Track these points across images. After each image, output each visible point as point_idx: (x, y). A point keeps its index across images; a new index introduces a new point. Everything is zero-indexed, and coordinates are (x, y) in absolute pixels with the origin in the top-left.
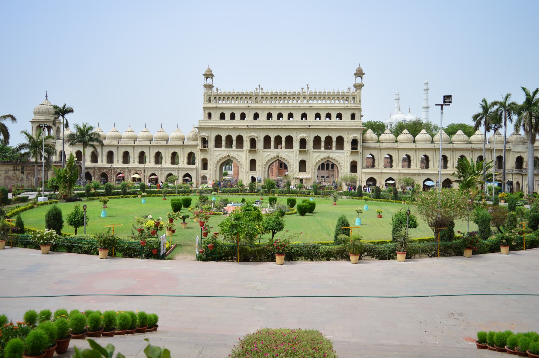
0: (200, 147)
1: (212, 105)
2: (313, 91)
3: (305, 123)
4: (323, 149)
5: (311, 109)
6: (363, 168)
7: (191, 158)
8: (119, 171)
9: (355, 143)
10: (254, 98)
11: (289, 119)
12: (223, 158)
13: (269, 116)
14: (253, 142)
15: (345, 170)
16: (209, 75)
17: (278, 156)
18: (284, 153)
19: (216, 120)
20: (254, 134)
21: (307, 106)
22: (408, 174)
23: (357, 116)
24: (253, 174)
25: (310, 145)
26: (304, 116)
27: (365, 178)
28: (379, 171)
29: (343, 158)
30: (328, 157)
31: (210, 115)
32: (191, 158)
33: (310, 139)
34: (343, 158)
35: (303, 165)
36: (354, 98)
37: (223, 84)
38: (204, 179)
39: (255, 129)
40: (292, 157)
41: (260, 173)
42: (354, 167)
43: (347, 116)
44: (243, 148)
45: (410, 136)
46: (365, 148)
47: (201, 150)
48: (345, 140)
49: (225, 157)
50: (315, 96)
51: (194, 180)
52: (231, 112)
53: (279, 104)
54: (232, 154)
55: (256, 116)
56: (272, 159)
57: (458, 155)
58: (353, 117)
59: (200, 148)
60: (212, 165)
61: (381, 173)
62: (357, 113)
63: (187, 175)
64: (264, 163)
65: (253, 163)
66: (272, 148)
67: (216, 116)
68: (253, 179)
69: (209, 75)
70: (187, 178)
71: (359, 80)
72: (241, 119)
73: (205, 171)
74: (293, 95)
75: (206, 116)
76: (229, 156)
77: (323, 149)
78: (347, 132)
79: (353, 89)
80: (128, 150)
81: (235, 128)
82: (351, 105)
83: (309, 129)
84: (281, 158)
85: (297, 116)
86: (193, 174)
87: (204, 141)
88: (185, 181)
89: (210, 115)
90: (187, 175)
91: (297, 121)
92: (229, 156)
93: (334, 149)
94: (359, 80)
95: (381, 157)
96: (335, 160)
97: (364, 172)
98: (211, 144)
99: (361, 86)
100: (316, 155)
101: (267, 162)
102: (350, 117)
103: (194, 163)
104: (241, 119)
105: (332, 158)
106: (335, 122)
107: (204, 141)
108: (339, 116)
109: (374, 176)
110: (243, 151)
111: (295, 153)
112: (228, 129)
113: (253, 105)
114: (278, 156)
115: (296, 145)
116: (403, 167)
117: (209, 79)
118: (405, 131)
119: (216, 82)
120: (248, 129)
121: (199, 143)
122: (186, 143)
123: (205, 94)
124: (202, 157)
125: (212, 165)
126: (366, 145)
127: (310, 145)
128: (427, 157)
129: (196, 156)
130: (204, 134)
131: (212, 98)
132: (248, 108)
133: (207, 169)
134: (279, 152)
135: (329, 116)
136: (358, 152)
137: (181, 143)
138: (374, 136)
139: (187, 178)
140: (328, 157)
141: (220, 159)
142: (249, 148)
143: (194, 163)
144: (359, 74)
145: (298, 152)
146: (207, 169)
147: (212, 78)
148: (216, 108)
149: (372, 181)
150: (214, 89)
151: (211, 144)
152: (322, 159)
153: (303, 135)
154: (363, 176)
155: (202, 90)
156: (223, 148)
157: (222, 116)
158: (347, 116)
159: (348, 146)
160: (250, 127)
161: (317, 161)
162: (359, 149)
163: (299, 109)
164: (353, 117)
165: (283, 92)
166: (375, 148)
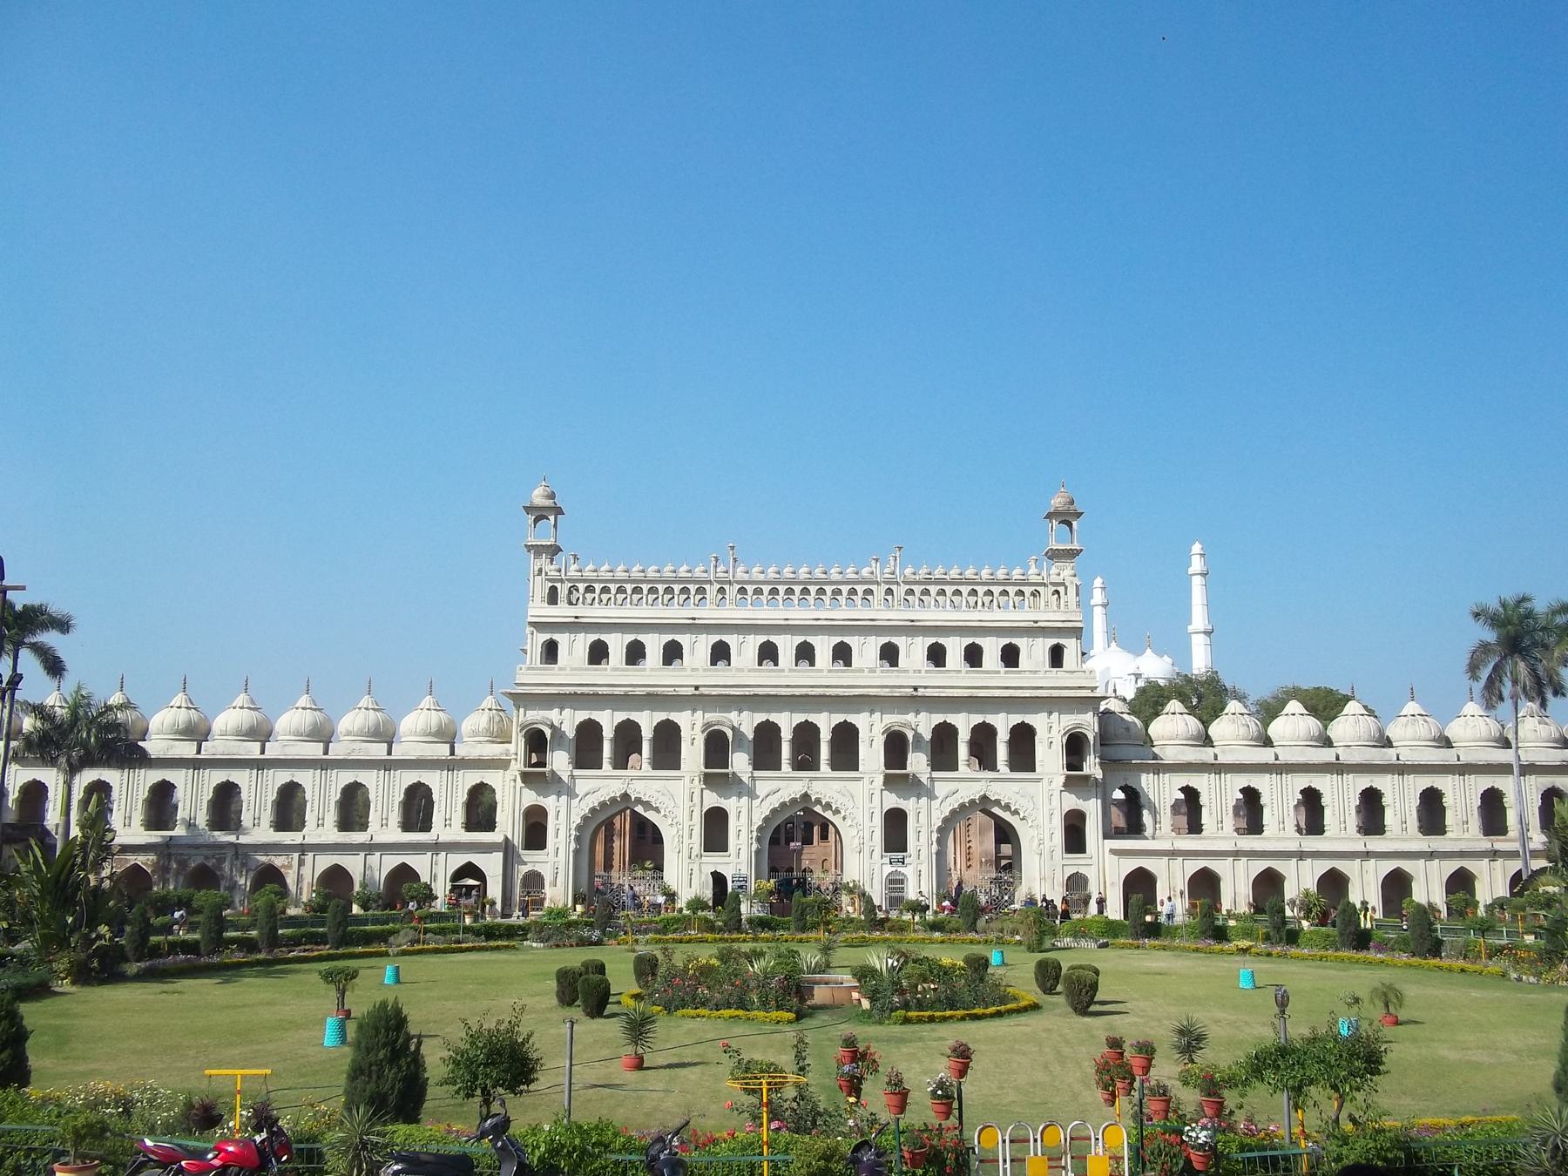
0: (518, 766)
1: (562, 612)
5: (913, 630)
6: (1105, 837)
7: (480, 810)
9: (1075, 746)
13: (768, 653)
21: (898, 615)
23: (1069, 657)
24: (715, 862)
26: (890, 654)
30: (984, 798)
32: (480, 810)
36: (1057, 592)
38: (534, 881)
41: (740, 859)
44: (678, 768)
45: (1193, 724)
49: (613, 800)
51: (494, 891)
53: (799, 614)
54: (638, 790)
55: (720, 653)
58: (1056, 656)
60: (744, 834)
63: (470, 870)
68: (719, 880)
70: (471, 882)
76: (626, 796)
81: (652, 700)
82: (1047, 613)
83: (916, 701)
85: (866, 651)
86: (491, 865)
87: (537, 742)
88: (457, 891)
90: (470, 870)
91: (872, 671)
92: (626, 796)
97: (1114, 852)
101: (766, 819)
102: (1045, 658)
103: (490, 826)
105: (997, 803)
108: (1010, 656)
109: (1149, 864)
111: (867, 786)
113: (708, 613)
116: (1177, 830)
118: (1174, 705)
120: (697, 700)
121: (517, 747)
122: (461, 751)
128: (1191, 794)
131: (563, 590)
132: (694, 627)
134: (812, 779)
136: (1087, 777)
137: (442, 751)
139: (471, 882)
140: (984, 798)
143: (490, 826)
145: (881, 778)
147: (555, 526)
148: (575, 626)
149: (1140, 885)
154: (1111, 860)
160: (703, 690)
164: (1056, 656)
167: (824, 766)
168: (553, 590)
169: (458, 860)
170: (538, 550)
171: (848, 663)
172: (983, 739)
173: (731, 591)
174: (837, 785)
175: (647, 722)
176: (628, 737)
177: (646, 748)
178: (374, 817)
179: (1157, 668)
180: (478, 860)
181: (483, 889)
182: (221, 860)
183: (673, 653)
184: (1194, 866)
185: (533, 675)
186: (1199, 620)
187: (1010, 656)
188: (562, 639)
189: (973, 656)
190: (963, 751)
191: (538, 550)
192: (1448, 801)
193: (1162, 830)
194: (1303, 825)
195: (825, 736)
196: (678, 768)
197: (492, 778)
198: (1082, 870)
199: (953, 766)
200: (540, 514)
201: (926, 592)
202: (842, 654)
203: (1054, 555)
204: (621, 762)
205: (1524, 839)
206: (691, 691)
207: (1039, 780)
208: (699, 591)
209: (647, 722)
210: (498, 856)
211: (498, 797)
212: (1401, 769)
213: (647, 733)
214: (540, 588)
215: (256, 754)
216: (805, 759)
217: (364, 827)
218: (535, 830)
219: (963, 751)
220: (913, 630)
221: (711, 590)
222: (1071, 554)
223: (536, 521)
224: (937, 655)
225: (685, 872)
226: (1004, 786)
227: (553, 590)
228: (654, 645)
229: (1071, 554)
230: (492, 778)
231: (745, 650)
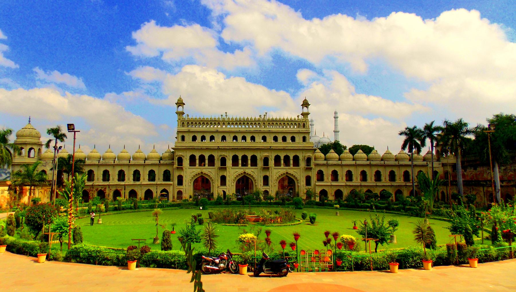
0: (176, 165)
1: (185, 129)
2: (271, 118)
4: (282, 166)
5: (270, 132)
7: (167, 176)
8: (100, 189)
9: (308, 160)
10: (221, 123)
12: (196, 175)
14: (223, 161)
15: (302, 183)
16: (180, 103)
19: (188, 142)
20: (224, 153)
22: (352, 186)
23: (307, 138)
24: (223, 188)
25: (272, 163)
26: (264, 139)
27: (318, 190)
28: (329, 184)
29: (298, 173)
30: (287, 173)
31: (183, 138)
35: (266, 180)
36: (304, 124)
37: (192, 111)
38: (180, 193)
39: (225, 149)
40: (255, 173)
43: (299, 138)
44: (214, 166)
48: (301, 158)
49: (199, 174)
50: (273, 122)
52: (202, 135)
54: (204, 171)
55: (224, 138)
56: (239, 175)
57: (389, 170)
58: (304, 139)
61: (331, 185)
62: (306, 135)
63: (165, 190)
64: (233, 177)
65: (223, 180)
66: (240, 166)
67: (188, 138)
69: (180, 103)
70: (164, 193)
71: (305, 110)
73: (181, 187)
74: (254, 121)
75: (180, 139)
76: (202, 173)
77: (282, 166)
78: (301, 152)
79: (301, 117)
80: (108, 168)
81: (208, 149)
82: (302, 129)
83: (270, 149)
84: (248, 174)
86: (170, 190)
88: (162, 195)
89: (183, 138)
90: (165, 190)
92: (202, 173)
94: (305, 110)
95: (327, 172)
96: (292, 175)
98: (186, 162)
99: (308, 114)
100: (276, 171)
102: (302, 139)
105: (290, 174)
106: (289, 143)
107: (180, 161)
108: (293, 139)
112: (201, 149)
114: (245, 173)
115: (260, 163)
117: (180, 107)
119: (186, 109)
120: (219, 149)
121: (176, 162)
123: (179, 119)
124: (177, 174)
125: (187, 181)
126: (317, 162)
127: (272, 163)
129: (171, 173)
130: (179, 154)
131: (186, 123)
132: (217, 132)
136: (311, 169)
138: (322, 155)
139: (164, 193)
140: (287, 173)
141: (194, 176)
144: (306, 104)
148: (189, 132)
149: (324, 193)
150: (184, 116)
151: (186, 162)
152: (282, 175)
153: (266, 154)
155: (176, 117)
156: (197, 165)
157: (194, 139)
158: (299, 138)
159: (303, 164)
161: (278, 176)
162: (312, 166)
163: (260, 132)
164: (304, 139)
165: (242, 118)
166: (323, 165)
167: (249, 166)
168: (183, 123)
171: (254, 141)
173: (226, 123)
175: (207, 155)
176: (202, 158)
180: (167, 188)
181: (167, 196)
182: (105, 188)
184: (336, 189)
188: (186, 135)
189: (284, 139)
190: (282, 162)
192: (396, 173)
193: (328, 180)
195: (249, 158)
196: (214, 166)
197: (169, 168)
199: (280, 165)
202: (253, 139)
204: (200, 165)
205: (413, 183)
206: (217, 148)
207: (300, 169)
209: (207, 155)
210: (172, 187)
212: (385, 166)
216: (245, 164)
218: (180, 181)
219: (282, 162)
224: (276, 139)
225: (217, 190)
226: (292, 170)
227: (183, 123)
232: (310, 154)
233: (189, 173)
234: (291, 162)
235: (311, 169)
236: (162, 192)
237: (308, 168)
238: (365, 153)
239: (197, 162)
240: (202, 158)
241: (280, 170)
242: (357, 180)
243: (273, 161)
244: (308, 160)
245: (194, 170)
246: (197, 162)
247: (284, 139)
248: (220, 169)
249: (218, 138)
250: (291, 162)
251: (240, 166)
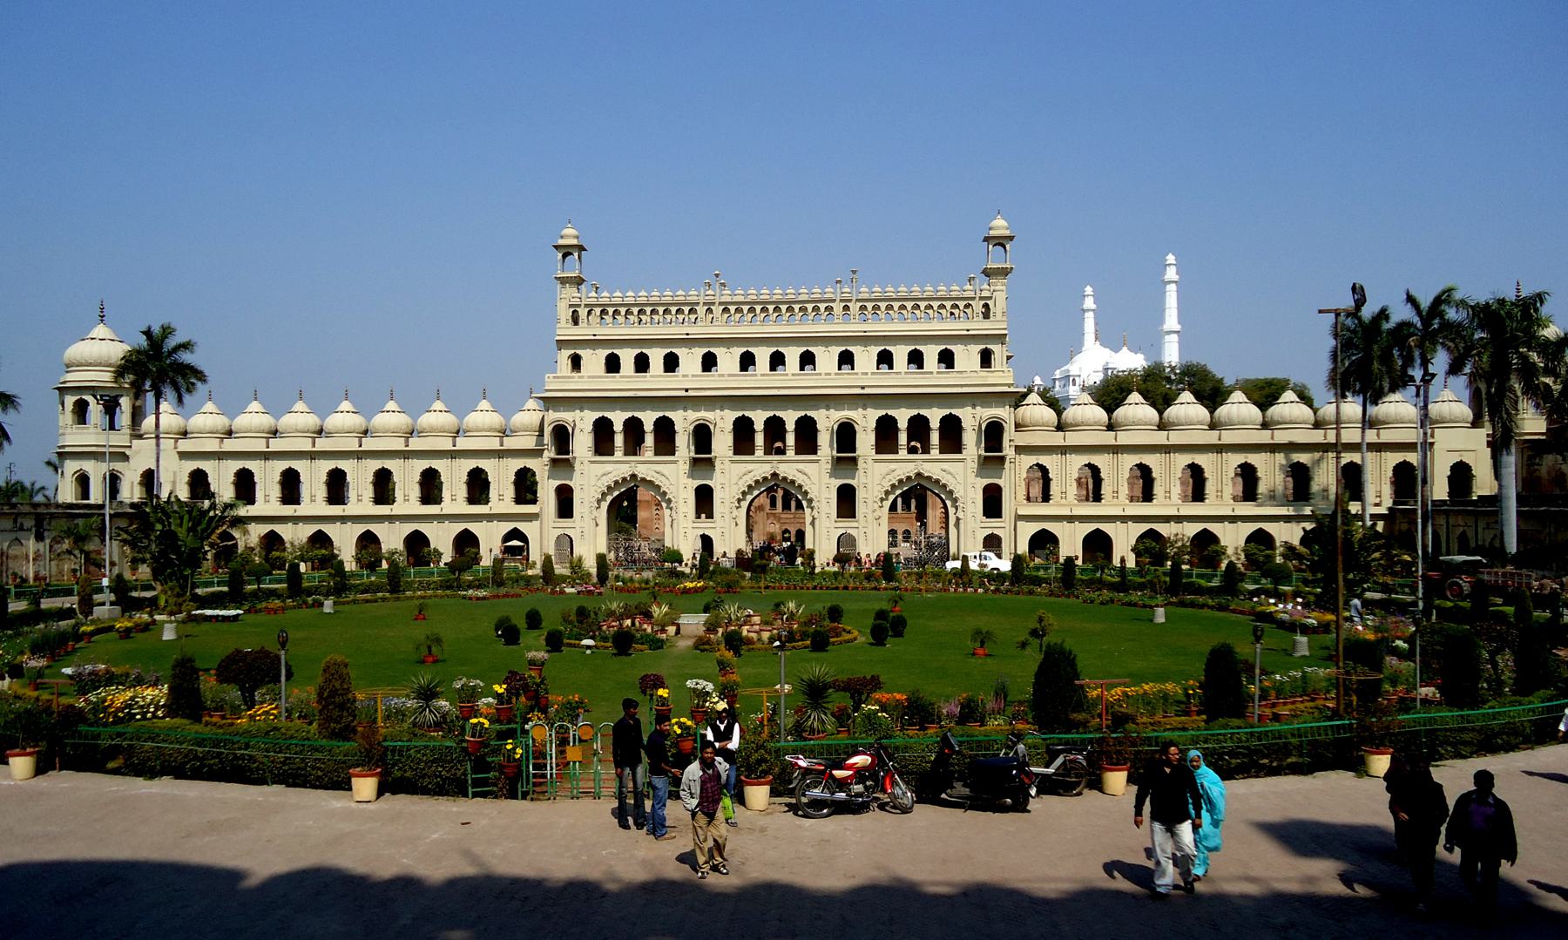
0: (550, 453)
1: (582, 332)
3: (846, 382)
4: (903, 453)
5: (865, 340)
7: (525, 487)
9: (993, 434)
11: (802, 369)
13: (747, 361)
17: (775, 475)
18: (792, 467)
26: (846, 359)
31: (576, 362)
33: (865, 421)
34: (960, 475)
36: (986, 306)
38: (566, 542)
40: (815, 476)
42: (992, 503)
46: (1020, 450)
47: (554, 461)
54: (643, 471)
55: (709, 362)
59: (553, 455)
63: (515, 534)
66: (759, 453)
68: (707, 542)
72: (666, 370)
73: (565, 522)
76: (634, 476)
77: (903, 453)
82: (979, 326)
89: (576, 362)
90: (515, 534)
92: (634, 476)
93: (935, 453)
96: (937, 481)
104: (666, 370)
105: (929, 478)
107: (562, 436)
108: (947, 359)
110: (675, 462)
114: (775, 475)
127: (865, 441)
133: (571, 516)
135: (916, 359)
140: (919, 475)
142: (693, 454)
146: (571, 516)
156: (619, 454)
157: (613, 364)
162: (1008, 451)
169: (508, 527)
170: (564, 281)
172: (919, 427)
174: (801, 466)
176: (634, 429)
177: (649, 440)
178: (446, 494)
179: (1130, 361)
180: (523, 527)
183: (671, 363)
185: (561, 380)
186: (1172, 321)
187: (947, 359)
189: (916, 359)
190: (903, 438)
191: (564, 281)
194: (1190, 492)
197: (531, 463)
198: (996, 532)
200: (567, 252)
201: (903, 307)
203: (987, 273)
208: (750, 310)
211: (538, 478)
213: (649, 426)
214: (565, 314)
215: (309, 448)
217: (437, 500)
220: (865, 340)
221: (701, 310)
222: (1005, 272)
223: (564, 256)
228: (656, 357)
229: (1005, 272)
230: (531, 463)
231: (728, 360)
232: (1003, 413)
233: (594, 477)
234: (935, 438)
235: (1002, 459)
236: (508, 537)
237: (992, 459)
238: (1153, 405)
239: (619, 440)
240: (634, 427)
241: (893, 466)
242: (1170, 498)
243: (872, 437)
244: (993, 434)
245: (609, 467)
246: (619, 440)
247: (642, 364)
248: (695, 462)
249: (690, 360)
250: (935, 438)
251: (759, 453)
